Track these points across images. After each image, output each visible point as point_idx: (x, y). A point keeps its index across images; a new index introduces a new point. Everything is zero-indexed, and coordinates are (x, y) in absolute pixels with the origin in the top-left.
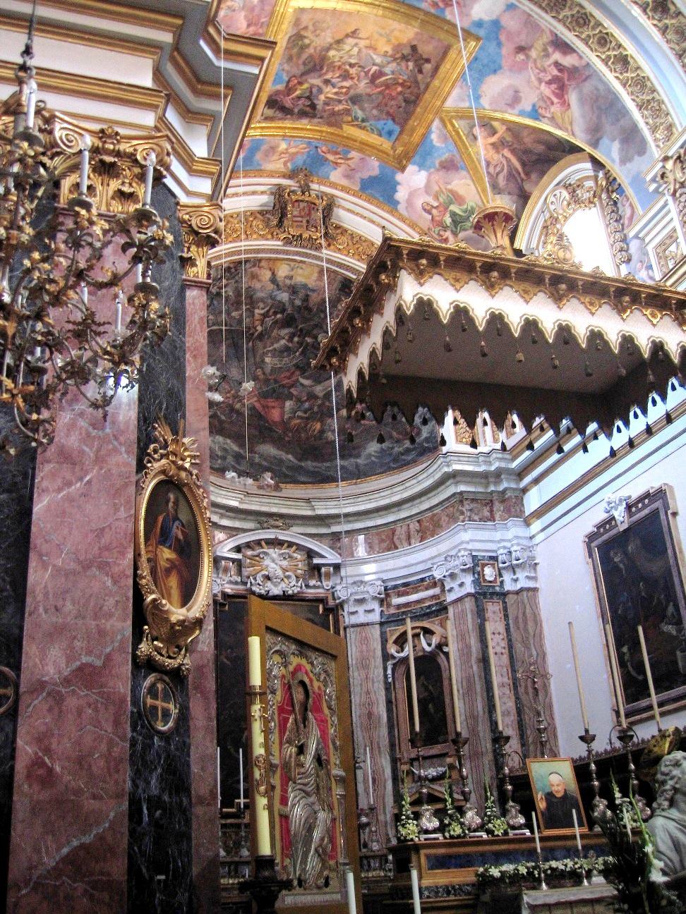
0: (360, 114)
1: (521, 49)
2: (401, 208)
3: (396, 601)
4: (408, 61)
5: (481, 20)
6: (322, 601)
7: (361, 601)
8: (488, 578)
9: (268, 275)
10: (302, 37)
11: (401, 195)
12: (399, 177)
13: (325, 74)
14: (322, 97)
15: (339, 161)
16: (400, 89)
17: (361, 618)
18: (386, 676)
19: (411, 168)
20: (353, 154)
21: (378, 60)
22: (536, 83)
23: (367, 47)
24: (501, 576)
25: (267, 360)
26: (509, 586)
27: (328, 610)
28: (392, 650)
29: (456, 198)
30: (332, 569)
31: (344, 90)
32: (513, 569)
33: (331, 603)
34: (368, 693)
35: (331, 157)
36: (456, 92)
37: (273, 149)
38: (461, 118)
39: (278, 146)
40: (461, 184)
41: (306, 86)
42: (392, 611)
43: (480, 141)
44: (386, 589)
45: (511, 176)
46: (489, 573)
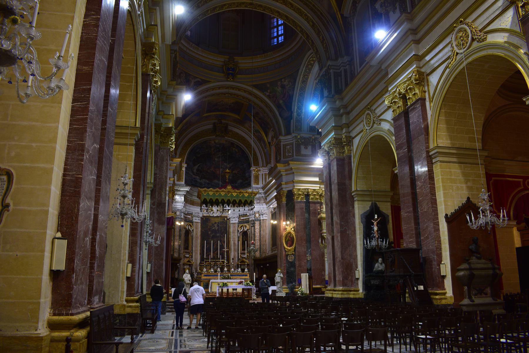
3: (242, 218)
6: (226, 217)
7: (234, 218)
8: (257, 216)
9: (213, 142)
17: (234, 222)
18: (238, 235)
24: (260, 215)
25: (216, 159)
26: (261, 218)
27: (227, 219)
28: (239, 230)
30: (227, 210)
32: (262, 215)
33: (228, 218)
34: (234, 238)
42: (241, 220)
44: (239, 215)
46: (257, 215)
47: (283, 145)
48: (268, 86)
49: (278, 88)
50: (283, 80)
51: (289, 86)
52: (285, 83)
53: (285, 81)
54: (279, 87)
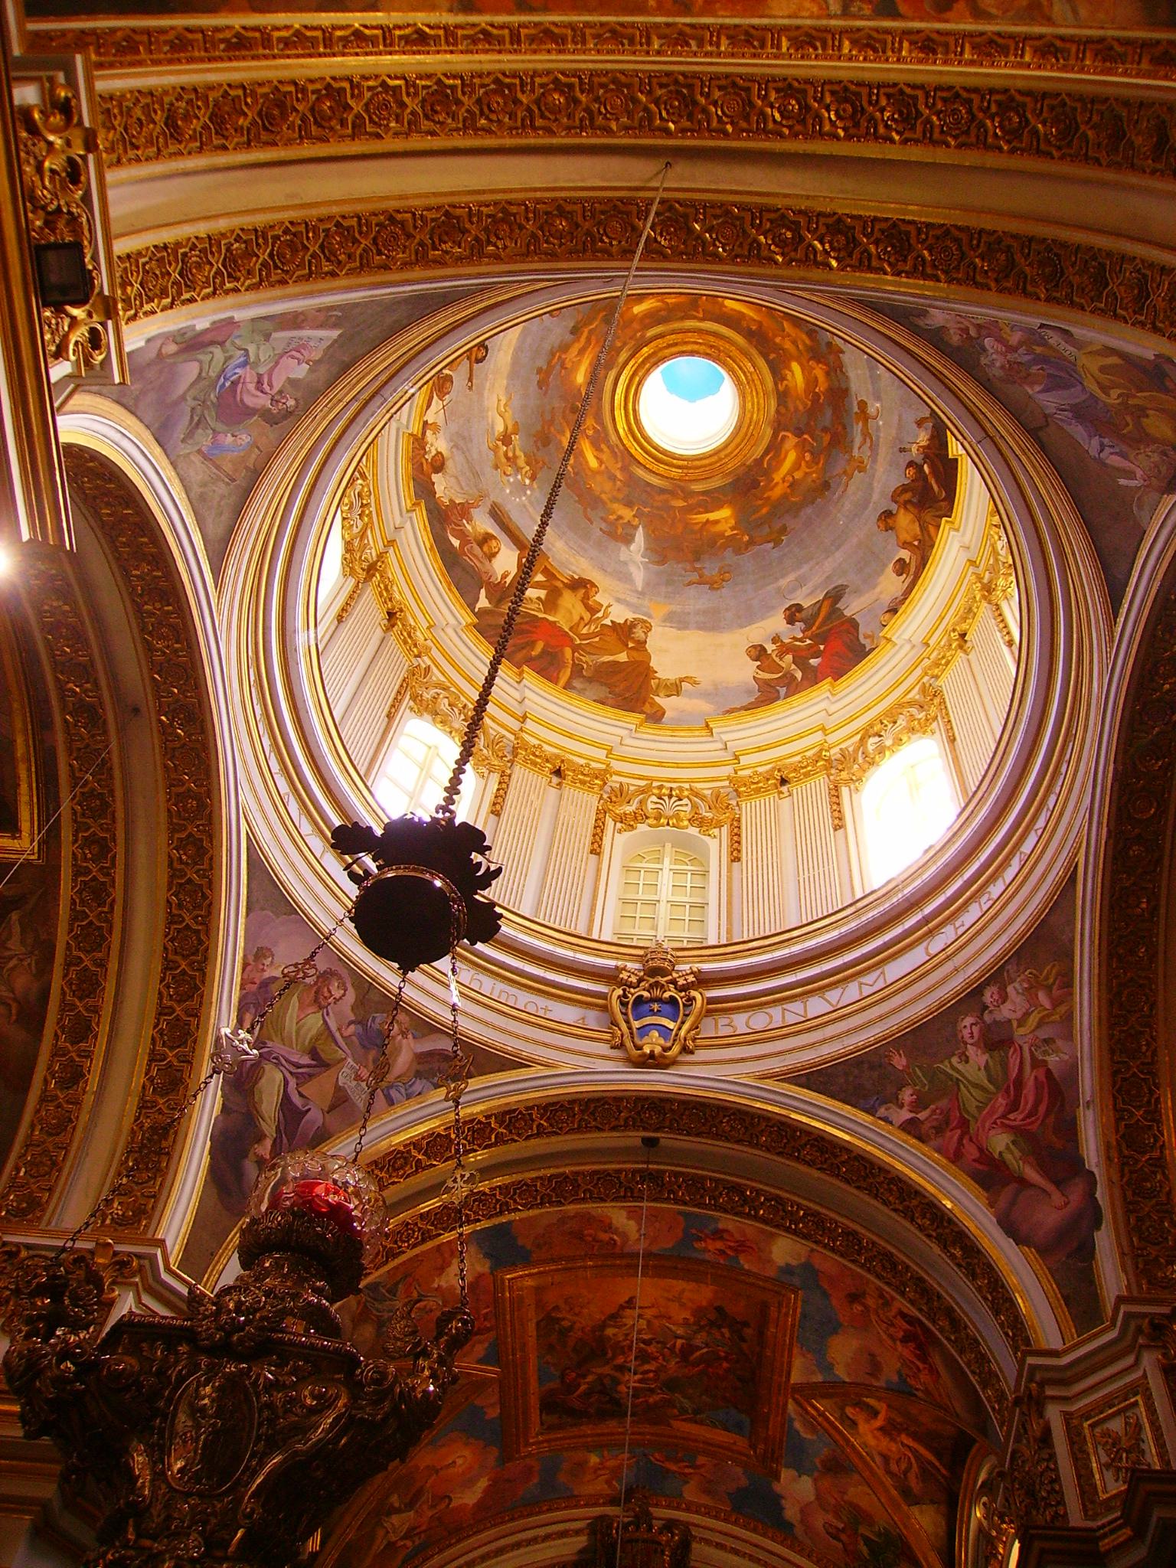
0: (687, 1403)
1: (854, 1298)
2: (799, 1531)
4: (719, 1327)
5: (787, 1265)
10: (559, 1320)
11: (791, 1513)
12: (777, 1487)
13: (614, 1357)
14: (622, 1388)
15: (687, 1471)
16: (725, 1365)
19: (786, 1474)
20: (701, 1460)
21: (680, 1331)
22: (890, 1342)
23: (656, 1317)
29: (859, 1516)
31: (651, 1375)
35: (673, 1467)
36: (798, 1362)
37: (582, 1465)
38: (824, 1396)
39: (587, 1461)
40: (857, 1493)
41: (590, 1378)
43: (863, 1427)
45: (926, 1472)
47: (1067, 1417)
48: (900, 1062)
49: (967, 1062)
50: (989, 996)
51: (1033, 1020)
52: (1006, 1012)
53: (1004, 998)
54: (971, 1051)
